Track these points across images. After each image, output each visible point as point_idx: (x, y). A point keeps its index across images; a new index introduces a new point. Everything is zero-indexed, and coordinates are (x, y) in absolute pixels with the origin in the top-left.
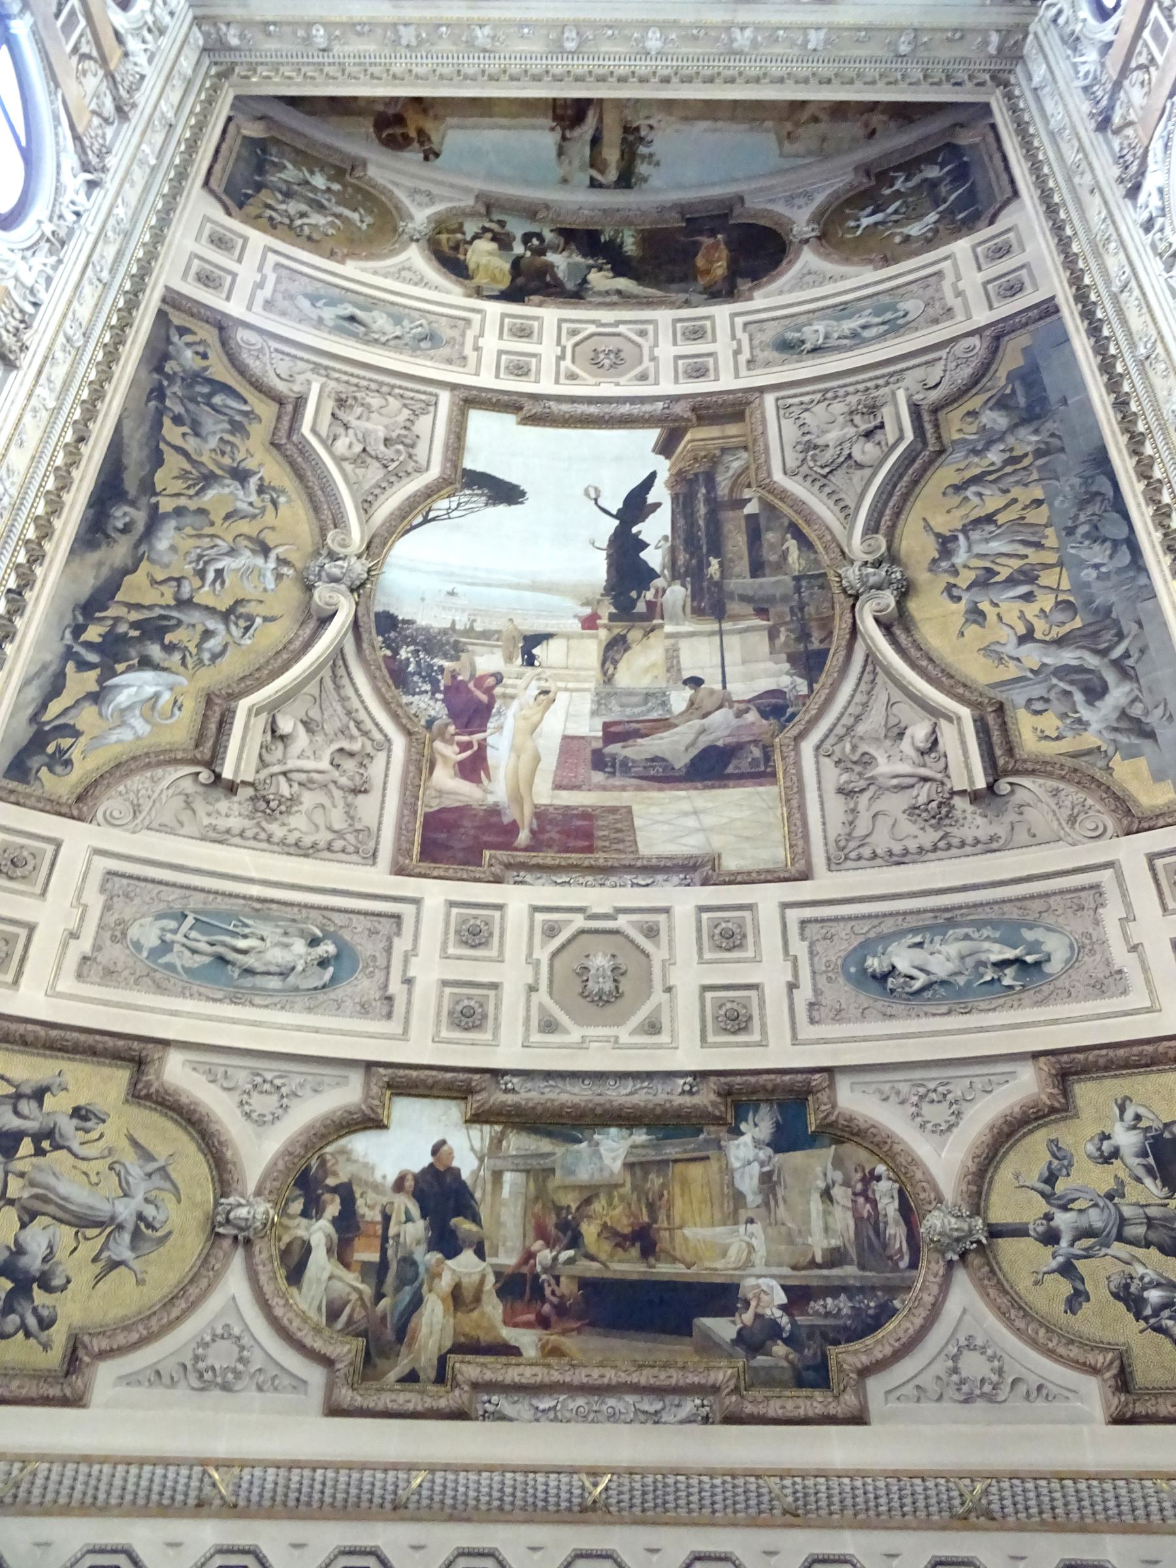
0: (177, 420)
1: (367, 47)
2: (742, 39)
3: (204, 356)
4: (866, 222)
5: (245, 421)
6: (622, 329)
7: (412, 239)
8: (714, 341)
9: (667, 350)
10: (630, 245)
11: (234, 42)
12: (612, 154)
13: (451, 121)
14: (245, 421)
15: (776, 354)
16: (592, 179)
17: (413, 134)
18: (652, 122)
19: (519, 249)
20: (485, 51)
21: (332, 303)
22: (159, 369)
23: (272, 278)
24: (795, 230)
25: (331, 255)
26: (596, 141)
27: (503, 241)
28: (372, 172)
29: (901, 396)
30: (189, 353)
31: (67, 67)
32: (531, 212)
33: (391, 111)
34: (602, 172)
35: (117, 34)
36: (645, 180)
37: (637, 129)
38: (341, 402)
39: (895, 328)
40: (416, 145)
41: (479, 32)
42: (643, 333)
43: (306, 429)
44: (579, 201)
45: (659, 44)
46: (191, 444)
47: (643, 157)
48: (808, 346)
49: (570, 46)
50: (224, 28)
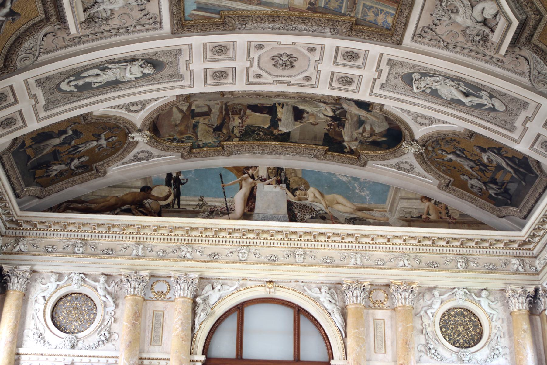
6: (271, 79)
8: (205, 70)
9: (240, 63)
11: (515, 261)
15: (162, 59)
21: (479, 106)
23: (518, 123)
24: (146, 139)
25: (472, 134)
29: (73, 30)
38: (485, 39)
39: (77, 73)
42: (259, 76)
43: (516, 23)
48: (137, 63)
50: (520, 269)
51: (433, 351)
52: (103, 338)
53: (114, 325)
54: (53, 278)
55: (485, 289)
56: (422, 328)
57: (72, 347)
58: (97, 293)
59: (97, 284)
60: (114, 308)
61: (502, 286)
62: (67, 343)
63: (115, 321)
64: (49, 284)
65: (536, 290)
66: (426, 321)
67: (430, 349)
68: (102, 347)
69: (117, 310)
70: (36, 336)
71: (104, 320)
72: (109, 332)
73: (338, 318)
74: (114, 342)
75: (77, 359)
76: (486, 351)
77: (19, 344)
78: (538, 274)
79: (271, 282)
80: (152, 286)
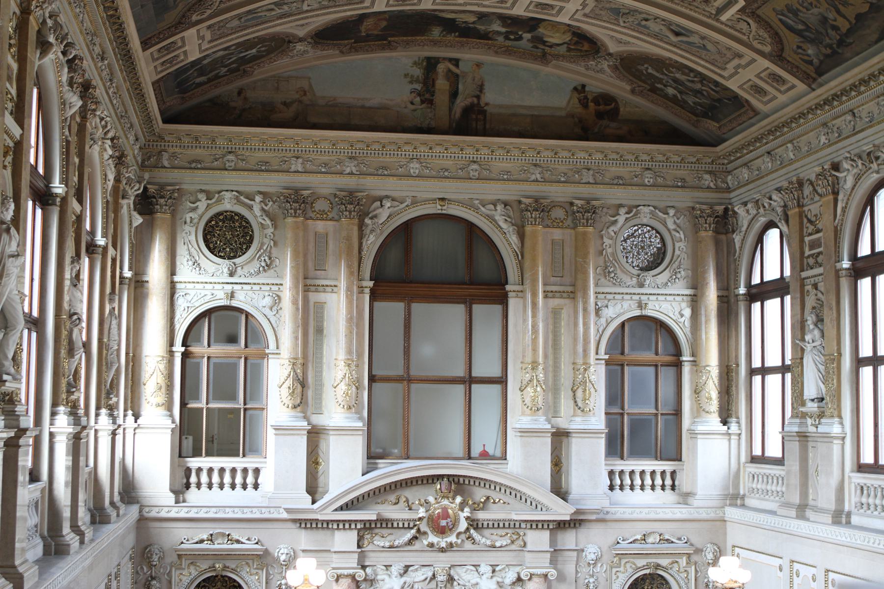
0: (835, 28)
1: (615, 170)
2: (350, 167)
3: (799, 47)
4: (254, 51)
5: (786, 12)
7: (610, 54)
10: (436, 32)
11: (707, 176)
12: (442, 84)
13: (563, 113)
14: (786, 12)
16: (457, 66)
17: (591, 105)
18: (413, 107)
19: (527, 36)
20: (535, 165)
22: (835, 53)
26: (454, 95)
27: (539, 40)
28: (628, 88)
30: (810, 52)
31: (826, 222)
32: (508, 52)
33: (605, 122)
34: (450, 70)
35: (787, 222)
36: (415, 63)
37: (422, 102)
40: (590, 97)
41: (538, 176)
44: (470, 55)
45: (412, 165)
46: (831, 15)
47: (417, 81)
49: (475, 166)
51: (613, 275)
52: (263, 264)
53: (273, 249)
54: (201, 196)
55: (673, 207)
56: (601, 249)
57: (231, 274)
58: (255, 215)
59: (252, 202)
60: (272, 230)
61: (691, 205)
62: (226, 270)
63: (275, 244)
64: (198, 203)
65: (726, 210)
66: (607, 241)
67: (609, 272)
68: (263, 274)
69: (277, 233)
70: (190, 263)
71: (262, 244)
72: (270, 258)
73: (514, 239)
74: (276, 269)
75: (236, 287)
76: (667, 274)
77: (173, 273)
78: (730, 192)
79: (443, 199)
80: (312, 204)
